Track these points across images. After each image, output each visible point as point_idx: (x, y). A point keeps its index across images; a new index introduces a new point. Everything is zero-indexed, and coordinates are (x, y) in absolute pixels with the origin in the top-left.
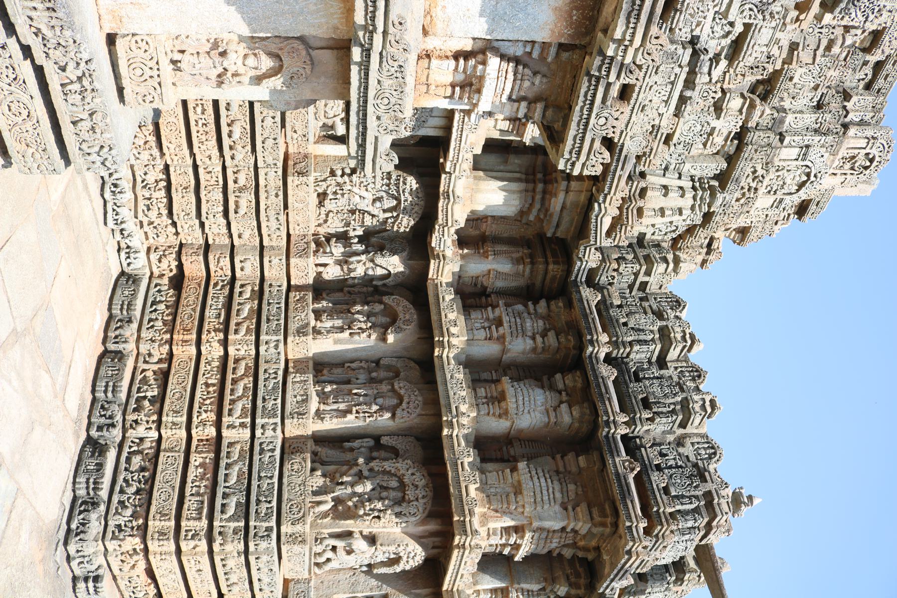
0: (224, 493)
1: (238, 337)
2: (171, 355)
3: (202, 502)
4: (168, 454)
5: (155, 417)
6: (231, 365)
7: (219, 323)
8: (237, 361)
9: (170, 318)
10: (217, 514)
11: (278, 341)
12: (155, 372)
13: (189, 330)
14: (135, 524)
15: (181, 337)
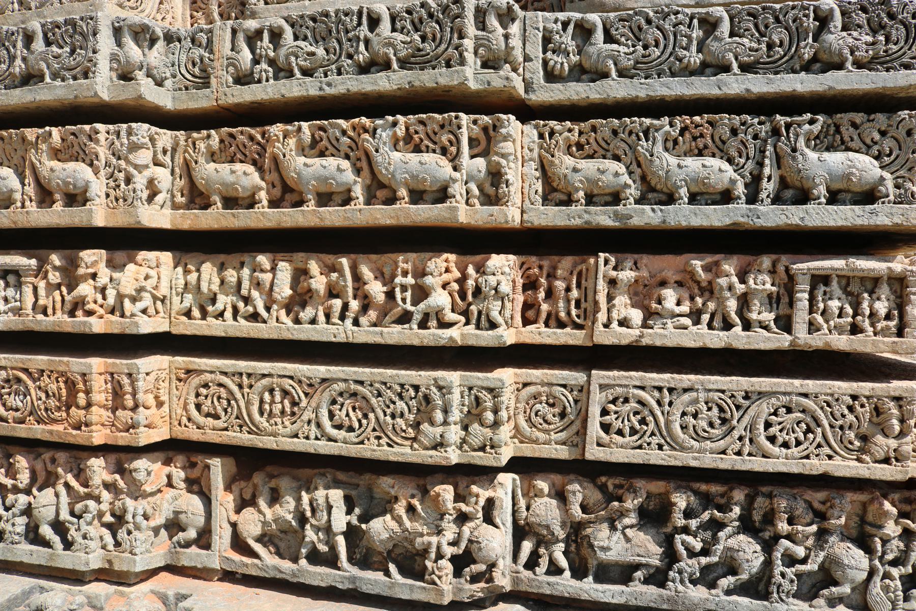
0: (777, 200)
1: (98, 187)
2: (169, 449)
3: (820, 280)
4: (594, 429)
5: (446, 492)
6: (215, 218)
7: (40, 272)
8: (197, 197)
9: (22, 462)
10: (882, 216)
11: (117, 32)
12: (242, 504)
13: (71, 385)
14: (892, 529)
15: (98, 414)
